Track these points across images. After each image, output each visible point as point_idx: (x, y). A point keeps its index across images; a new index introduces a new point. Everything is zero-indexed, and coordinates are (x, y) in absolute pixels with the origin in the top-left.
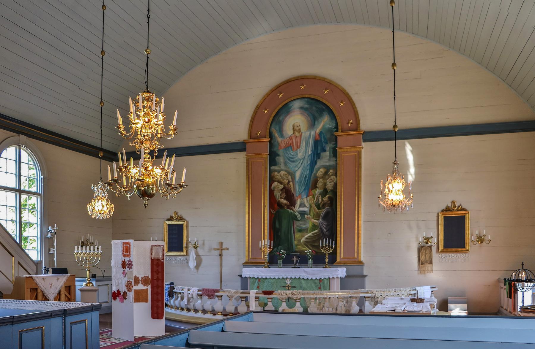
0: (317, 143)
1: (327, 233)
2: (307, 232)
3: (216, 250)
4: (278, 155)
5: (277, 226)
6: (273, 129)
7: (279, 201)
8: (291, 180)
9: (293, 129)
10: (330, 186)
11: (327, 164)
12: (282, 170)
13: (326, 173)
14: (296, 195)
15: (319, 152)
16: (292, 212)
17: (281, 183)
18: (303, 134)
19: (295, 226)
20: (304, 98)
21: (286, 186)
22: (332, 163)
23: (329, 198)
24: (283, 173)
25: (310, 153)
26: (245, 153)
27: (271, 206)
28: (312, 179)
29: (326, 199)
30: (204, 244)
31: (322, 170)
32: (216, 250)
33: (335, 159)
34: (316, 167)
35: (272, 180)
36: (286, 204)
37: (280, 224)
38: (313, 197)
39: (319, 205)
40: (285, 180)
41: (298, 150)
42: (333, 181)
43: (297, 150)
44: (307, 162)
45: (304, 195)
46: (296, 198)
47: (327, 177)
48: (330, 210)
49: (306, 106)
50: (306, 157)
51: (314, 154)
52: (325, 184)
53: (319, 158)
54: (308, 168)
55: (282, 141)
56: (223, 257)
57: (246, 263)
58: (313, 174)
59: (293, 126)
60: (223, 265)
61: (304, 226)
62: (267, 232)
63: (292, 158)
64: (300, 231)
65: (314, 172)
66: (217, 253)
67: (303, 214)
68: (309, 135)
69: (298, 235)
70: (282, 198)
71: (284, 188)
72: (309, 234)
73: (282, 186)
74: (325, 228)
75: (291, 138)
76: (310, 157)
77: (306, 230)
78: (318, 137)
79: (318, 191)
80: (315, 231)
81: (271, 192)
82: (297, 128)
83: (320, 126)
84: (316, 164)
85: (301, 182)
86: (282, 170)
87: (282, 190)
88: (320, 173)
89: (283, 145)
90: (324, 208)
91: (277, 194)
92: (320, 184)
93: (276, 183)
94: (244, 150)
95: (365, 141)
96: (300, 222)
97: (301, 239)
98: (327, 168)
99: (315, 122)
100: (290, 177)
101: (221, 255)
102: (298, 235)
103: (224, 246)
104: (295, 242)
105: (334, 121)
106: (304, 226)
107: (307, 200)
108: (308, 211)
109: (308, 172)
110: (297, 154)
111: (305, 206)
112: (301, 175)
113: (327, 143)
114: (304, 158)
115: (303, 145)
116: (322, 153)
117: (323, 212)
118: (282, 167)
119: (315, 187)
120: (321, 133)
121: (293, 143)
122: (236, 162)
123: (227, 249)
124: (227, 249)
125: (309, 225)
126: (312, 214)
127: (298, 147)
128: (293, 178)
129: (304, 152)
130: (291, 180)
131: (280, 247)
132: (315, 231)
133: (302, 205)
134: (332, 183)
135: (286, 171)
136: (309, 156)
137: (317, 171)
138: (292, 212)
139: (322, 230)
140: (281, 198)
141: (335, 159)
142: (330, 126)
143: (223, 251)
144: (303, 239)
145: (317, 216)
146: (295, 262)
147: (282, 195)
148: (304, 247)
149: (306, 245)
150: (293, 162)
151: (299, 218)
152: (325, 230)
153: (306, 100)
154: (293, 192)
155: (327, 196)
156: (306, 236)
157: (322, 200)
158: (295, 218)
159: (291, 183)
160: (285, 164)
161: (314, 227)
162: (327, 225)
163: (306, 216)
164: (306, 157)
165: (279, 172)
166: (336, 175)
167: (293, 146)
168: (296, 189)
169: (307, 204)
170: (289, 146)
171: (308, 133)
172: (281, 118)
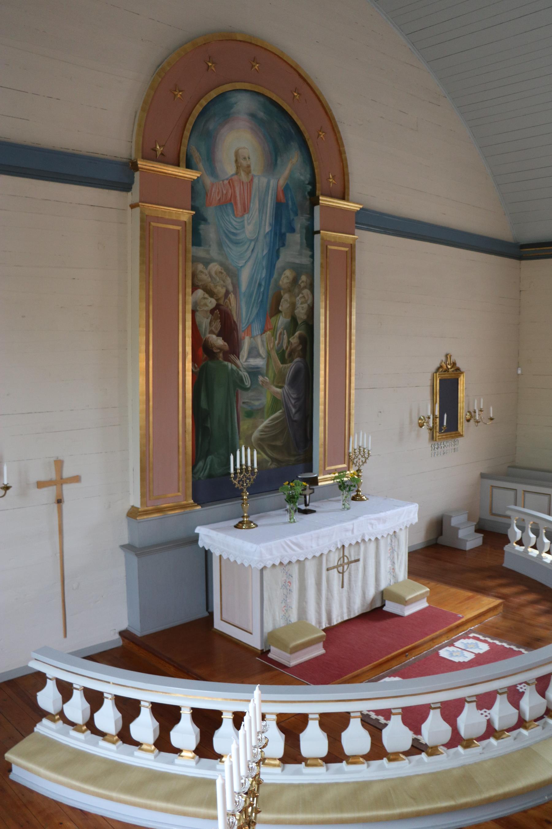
0: (280, 208)
2: (263, 418)
3: (40, 485)
4: (205, 220)
7: (206, 341)
8: (231, 288)
9: (236, 161)
10: (301, 312)
11: (297, 261)
12: (212, 260)
13: (295, 281)
14: (242, 326)
15: (283, 230)
16: (235, 368)
17: (210, 293)
18: (256, 180)
19: (240, 403)
20: (258, 94)
21: (221, 302)
22: (305, 261)
23: (301, 337)
24: (214, 267)
25: (268, 229)
28: (271, 293)
29: (294, 340)
31: (288, 274)
32: (40, 485)
33: (310, 253)
34: (279, 264)
36: (221, 349)
38: (273, 335)
39: (284, 352)
40: (219, 288)
41: (246, 216)
42: (306, 302)
43: (242, 216)
44: (262, 250)
45: (256, 329)
46: (241, 334)
47: (297, 290)
48: (302, 365)
49: (261, 114)
50: (261, 238)
51: (275, 234)
52: (293, 306)
53: (283, 245)
54: (264, 263)
55: (213, 185)
58: (273, 280)
59: (237, 154)
60: (65, 527)
61: (257, 403)
63: (234, 234)
64: (250, 414)
65: (275, 276)
67: (254, 372)
68: (266, 185)
69: (245, 424)
70: (214, 333)
71: (218, 306)
72: (266, 422)
74: (294, 406)
75: (231, 182)
76: (268, 239)
78: (281, 195)
79: (282, 321)
80: (277, 414)
82: (244, 163)
83: (286, 173)
84: (278, 257)
85: (251, 296)
86: (212, 260)
87: (212, 311)
88: (286, 281)
89: (215, 196)
90: (291, 361)
92: (284, 306)
96: (251, 394)
98: (298, 270)
99: (276, 160)
100: (229, 281)
105: (308, 169)
106: (257, 403)
107: (262, 341)
108: (265, 367)
109: (264, 275)
110: (244, 227)
111: (258, 355)
112: (252, 279)
113: (296, 214)
114: (256, 240)
115: (255, 206)
116: (288, 235)
117: (290, 368)
118: (214, 253)
119: (276, 311)
120: (287, 188)
121: (235, 197)
125: (266, 400)
127: (246, 210)
128: (236, 285)
129: (254, 224)
130: (231, 288)
132: (277, 414)
133: (253, 352)
134: (305, 306)
135: (222, 264)
136: (265, 237)
137: (280, 275)
138: (235, 368)
139: (288, 410)
140: (211, 332)
141: (310, 253)
142: (302, 178)
144: (256, 434)
145: (279, 381)
147: (214, 324)
150: (236, 243)
151: (248, 383)
153: (262, 99)
154: (235, 319)
155: (297, 334)
156: (261, 427)
157: (289, 342)
159: (232, 297)
160: (220, 245)
161: (276, 403)
162: (297, 399)
163: (260, 378)
164: (261, 238)
165: (206, 263)
167: (236, 203)
168: (243, 312)
169: (262, 351)
170: (227, 203)
171: (264, 180)
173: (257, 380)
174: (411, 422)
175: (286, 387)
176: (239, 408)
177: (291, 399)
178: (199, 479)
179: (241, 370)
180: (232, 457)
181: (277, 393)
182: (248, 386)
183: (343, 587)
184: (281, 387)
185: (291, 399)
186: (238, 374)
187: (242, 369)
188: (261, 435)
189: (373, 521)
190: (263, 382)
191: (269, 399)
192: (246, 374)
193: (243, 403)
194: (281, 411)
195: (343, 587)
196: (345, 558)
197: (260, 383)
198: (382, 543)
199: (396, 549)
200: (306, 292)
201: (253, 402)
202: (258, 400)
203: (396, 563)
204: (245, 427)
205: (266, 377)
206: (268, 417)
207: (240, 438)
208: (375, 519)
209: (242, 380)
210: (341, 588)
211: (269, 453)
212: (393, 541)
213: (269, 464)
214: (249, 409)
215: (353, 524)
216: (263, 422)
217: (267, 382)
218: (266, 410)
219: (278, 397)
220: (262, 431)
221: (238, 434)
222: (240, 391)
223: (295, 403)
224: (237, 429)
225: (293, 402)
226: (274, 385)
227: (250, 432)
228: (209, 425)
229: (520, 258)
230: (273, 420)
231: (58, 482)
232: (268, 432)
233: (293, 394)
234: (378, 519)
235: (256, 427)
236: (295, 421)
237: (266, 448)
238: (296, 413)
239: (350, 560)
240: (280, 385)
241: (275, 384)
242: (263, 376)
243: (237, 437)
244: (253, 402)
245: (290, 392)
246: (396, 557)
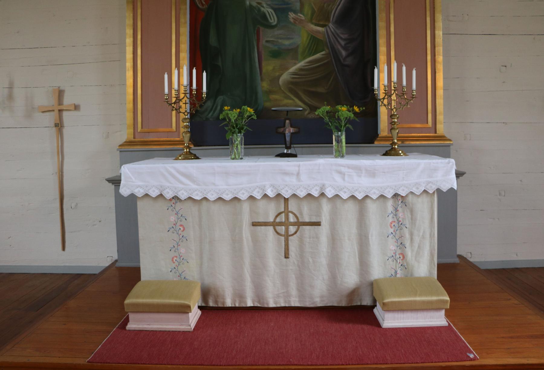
1: (349, 61)
2: (296, 59)
5: (213, 41)
19: (263, 42)
56: (65, 131)
57: (129, 143)
61: (287, 42)
64: (276, 54)
66: (49, 119)
69: (269, 66)
72: (301, 64)
74: (345, 48)
77: (292, 53)
80: (318, 56)
101: (59, 126)
102: (269, 66)
103: (68, 100)
104: (264, 85)
106: (287, 42)
123: (77, 108)
124: (77, 108)
125: (301, 39)
126: (307, 9)
131: (220, 99)
132: (318, 56)
139: (334, 52)
143: (65, 114)
144: (285, 77)
146: (288, 139)
148: (288, 98)
149: (291, 91)
151: (273, 20)
152: (344, 53)
156: (293, 69)
161: (315, 44)
163: (292, 15)
173: (287, 17)
175: (331, 25)
176: (260, 46)
177: (340, 40)
178: (207, 119)
179: (263, 7)
180: (166, 76)
181: (318, 32)
182: (275, 23)
183: (287, 256)
184: (322, 26)
185: (340, 40)
186: (259, 10)
187: (265, 5)
188: (293, 78)
189: (343, 169)
190: (295, 19)
191: (305, 39)
192: (270, 10)
193: (267, 41)
194: (323, 53)
195: (287, 256)
196: (291, 215)
197: (292, 20)
198: (372, 208)
199: (407, 223)
201: (280, 41)
202: (288, 39)
203: (408, 244)
204: (270, 68)
205: (299, 14)
206: (304, 58)
207: (262, 80)
208: (349, 167)
209: (264, 16)
210: (283, 258)
211: (306, 100)
212: (399, 209)
213: (307, 112)
214: (276, 48)
215: (299, 166)
216: (295, 64)
217: (301, 20)
218: (300, 50)
219: (320, 37)
220: (294, 74)
221: (259, 74)
222: (261, 28)
223: (345, 44)
224: (258, 70)
225: (343, 43)
226: (312, 23)
227: (277, 74)
228: (220, 64)
230: (310, 62)
232: (304, 75)
233: (343, 34)
234: (358, 169)
235: (287, 69)
236: (347, 66)
237: (300, 93)
238: (347, 56)
239: (301, 220)
240: (321, 23)
241: (314, 21)
242: (295, 12)
243: (259, 78)
244: (280, 41)
245: (338, 32)
246: (407, 236)
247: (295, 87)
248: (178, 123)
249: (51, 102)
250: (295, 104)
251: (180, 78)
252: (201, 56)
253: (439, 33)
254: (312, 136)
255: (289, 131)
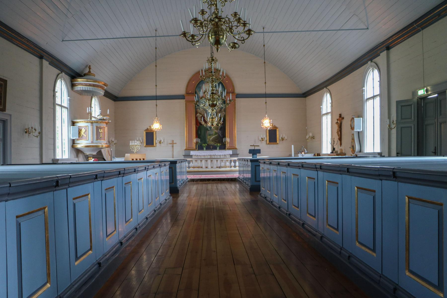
3: (170, 144)
5: (199, 133)
6: (197, 90)
26: (185, 100)
27: (196, 124)
30: (164, 141)
32: (170, 144)
35: (196, 113)
37: (201, 132)
57: (186, 149)
62: (195, 135)
64: (210, 135)
66: (171, 145)
69: (208, 137)
73: (201, 116)
77: (212, 135)
81: (196, 118)
91: (199, 119)
93: (198, 114)
94: (184, 99)
95: (237, 97)
97: (210, 139)
101: (173, 146)
102: (208, 137)
103: (174, 142)
104: (208, 140)
122: (180, 104)
123: (176, 143)
124: (176, 143)
125: (214, 133)
139: (219, 135)
144: (211, 139)
151: (209, 129)
158: (207, 130)
161: (216, 133)
166: (225, 111)
172: (200, 86)
174: (258, 139)
200: (224, 112)
229: (305, 97)
231: (173, 143)
247: (212, 140)
248: (194, 146)
249: (172, 142)
250: (212, 143)
251: (195, 140)
252: (198, 135)
253: (236, 132)
254: (215, 148)
255: (211, 147)
